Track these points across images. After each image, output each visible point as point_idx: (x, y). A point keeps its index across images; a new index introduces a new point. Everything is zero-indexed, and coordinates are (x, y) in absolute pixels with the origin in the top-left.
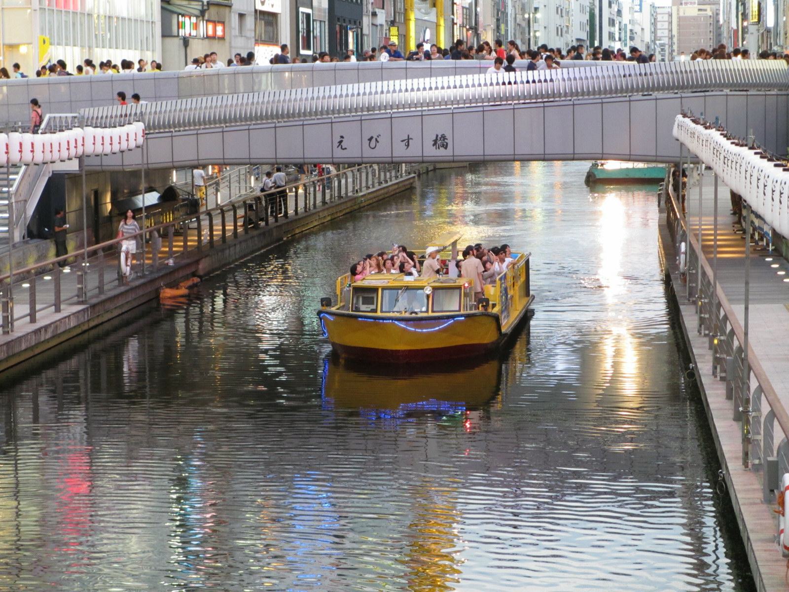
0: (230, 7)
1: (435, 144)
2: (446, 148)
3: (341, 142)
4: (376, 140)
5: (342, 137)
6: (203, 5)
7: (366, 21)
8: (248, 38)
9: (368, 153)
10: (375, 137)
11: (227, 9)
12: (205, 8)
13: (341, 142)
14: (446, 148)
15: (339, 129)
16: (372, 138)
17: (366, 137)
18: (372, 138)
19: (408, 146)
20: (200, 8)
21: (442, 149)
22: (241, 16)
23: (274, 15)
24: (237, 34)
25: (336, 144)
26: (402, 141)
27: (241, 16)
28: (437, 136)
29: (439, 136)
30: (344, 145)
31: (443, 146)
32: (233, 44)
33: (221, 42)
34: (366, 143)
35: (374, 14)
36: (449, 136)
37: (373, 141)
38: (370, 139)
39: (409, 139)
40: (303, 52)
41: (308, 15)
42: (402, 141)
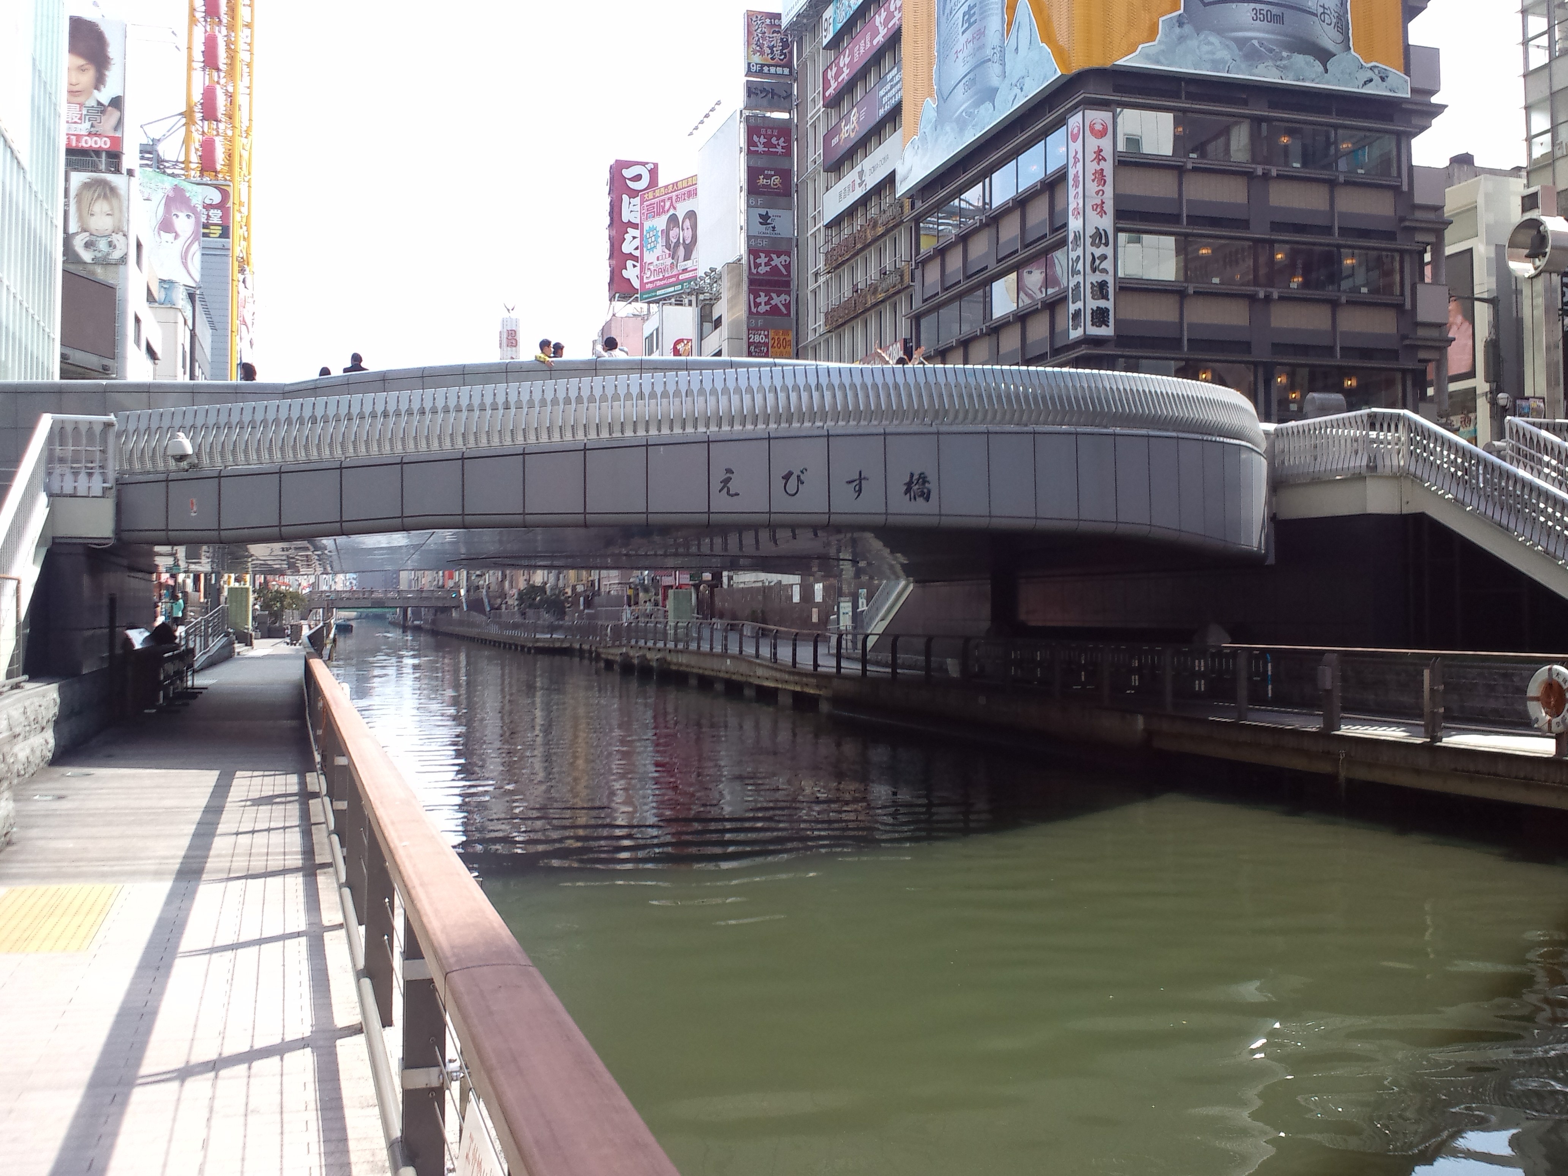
1: (908, 491)
2: (927, 499)
3: (726, 481)
4: (798, 477)
5: (729, 471)
9: (783, 504)
10: (796, 473)
13: (726, 481)
14: (927, 499)
15: (722, 457)
16: (790, 474)
17: (778, 473)
18: (790, 474)
19: (860, 491)
21: (920, 500)
25: (716, 485)
26: (850, 482)
28: (912, 475)
29: (916, 477)
30: (733, 486)
31: (922, 494)
34: (778, 483)
36: (932, 477)
37: (793, 482)
38: (787, 477)
39: (860, 479)
42: (850, 482)
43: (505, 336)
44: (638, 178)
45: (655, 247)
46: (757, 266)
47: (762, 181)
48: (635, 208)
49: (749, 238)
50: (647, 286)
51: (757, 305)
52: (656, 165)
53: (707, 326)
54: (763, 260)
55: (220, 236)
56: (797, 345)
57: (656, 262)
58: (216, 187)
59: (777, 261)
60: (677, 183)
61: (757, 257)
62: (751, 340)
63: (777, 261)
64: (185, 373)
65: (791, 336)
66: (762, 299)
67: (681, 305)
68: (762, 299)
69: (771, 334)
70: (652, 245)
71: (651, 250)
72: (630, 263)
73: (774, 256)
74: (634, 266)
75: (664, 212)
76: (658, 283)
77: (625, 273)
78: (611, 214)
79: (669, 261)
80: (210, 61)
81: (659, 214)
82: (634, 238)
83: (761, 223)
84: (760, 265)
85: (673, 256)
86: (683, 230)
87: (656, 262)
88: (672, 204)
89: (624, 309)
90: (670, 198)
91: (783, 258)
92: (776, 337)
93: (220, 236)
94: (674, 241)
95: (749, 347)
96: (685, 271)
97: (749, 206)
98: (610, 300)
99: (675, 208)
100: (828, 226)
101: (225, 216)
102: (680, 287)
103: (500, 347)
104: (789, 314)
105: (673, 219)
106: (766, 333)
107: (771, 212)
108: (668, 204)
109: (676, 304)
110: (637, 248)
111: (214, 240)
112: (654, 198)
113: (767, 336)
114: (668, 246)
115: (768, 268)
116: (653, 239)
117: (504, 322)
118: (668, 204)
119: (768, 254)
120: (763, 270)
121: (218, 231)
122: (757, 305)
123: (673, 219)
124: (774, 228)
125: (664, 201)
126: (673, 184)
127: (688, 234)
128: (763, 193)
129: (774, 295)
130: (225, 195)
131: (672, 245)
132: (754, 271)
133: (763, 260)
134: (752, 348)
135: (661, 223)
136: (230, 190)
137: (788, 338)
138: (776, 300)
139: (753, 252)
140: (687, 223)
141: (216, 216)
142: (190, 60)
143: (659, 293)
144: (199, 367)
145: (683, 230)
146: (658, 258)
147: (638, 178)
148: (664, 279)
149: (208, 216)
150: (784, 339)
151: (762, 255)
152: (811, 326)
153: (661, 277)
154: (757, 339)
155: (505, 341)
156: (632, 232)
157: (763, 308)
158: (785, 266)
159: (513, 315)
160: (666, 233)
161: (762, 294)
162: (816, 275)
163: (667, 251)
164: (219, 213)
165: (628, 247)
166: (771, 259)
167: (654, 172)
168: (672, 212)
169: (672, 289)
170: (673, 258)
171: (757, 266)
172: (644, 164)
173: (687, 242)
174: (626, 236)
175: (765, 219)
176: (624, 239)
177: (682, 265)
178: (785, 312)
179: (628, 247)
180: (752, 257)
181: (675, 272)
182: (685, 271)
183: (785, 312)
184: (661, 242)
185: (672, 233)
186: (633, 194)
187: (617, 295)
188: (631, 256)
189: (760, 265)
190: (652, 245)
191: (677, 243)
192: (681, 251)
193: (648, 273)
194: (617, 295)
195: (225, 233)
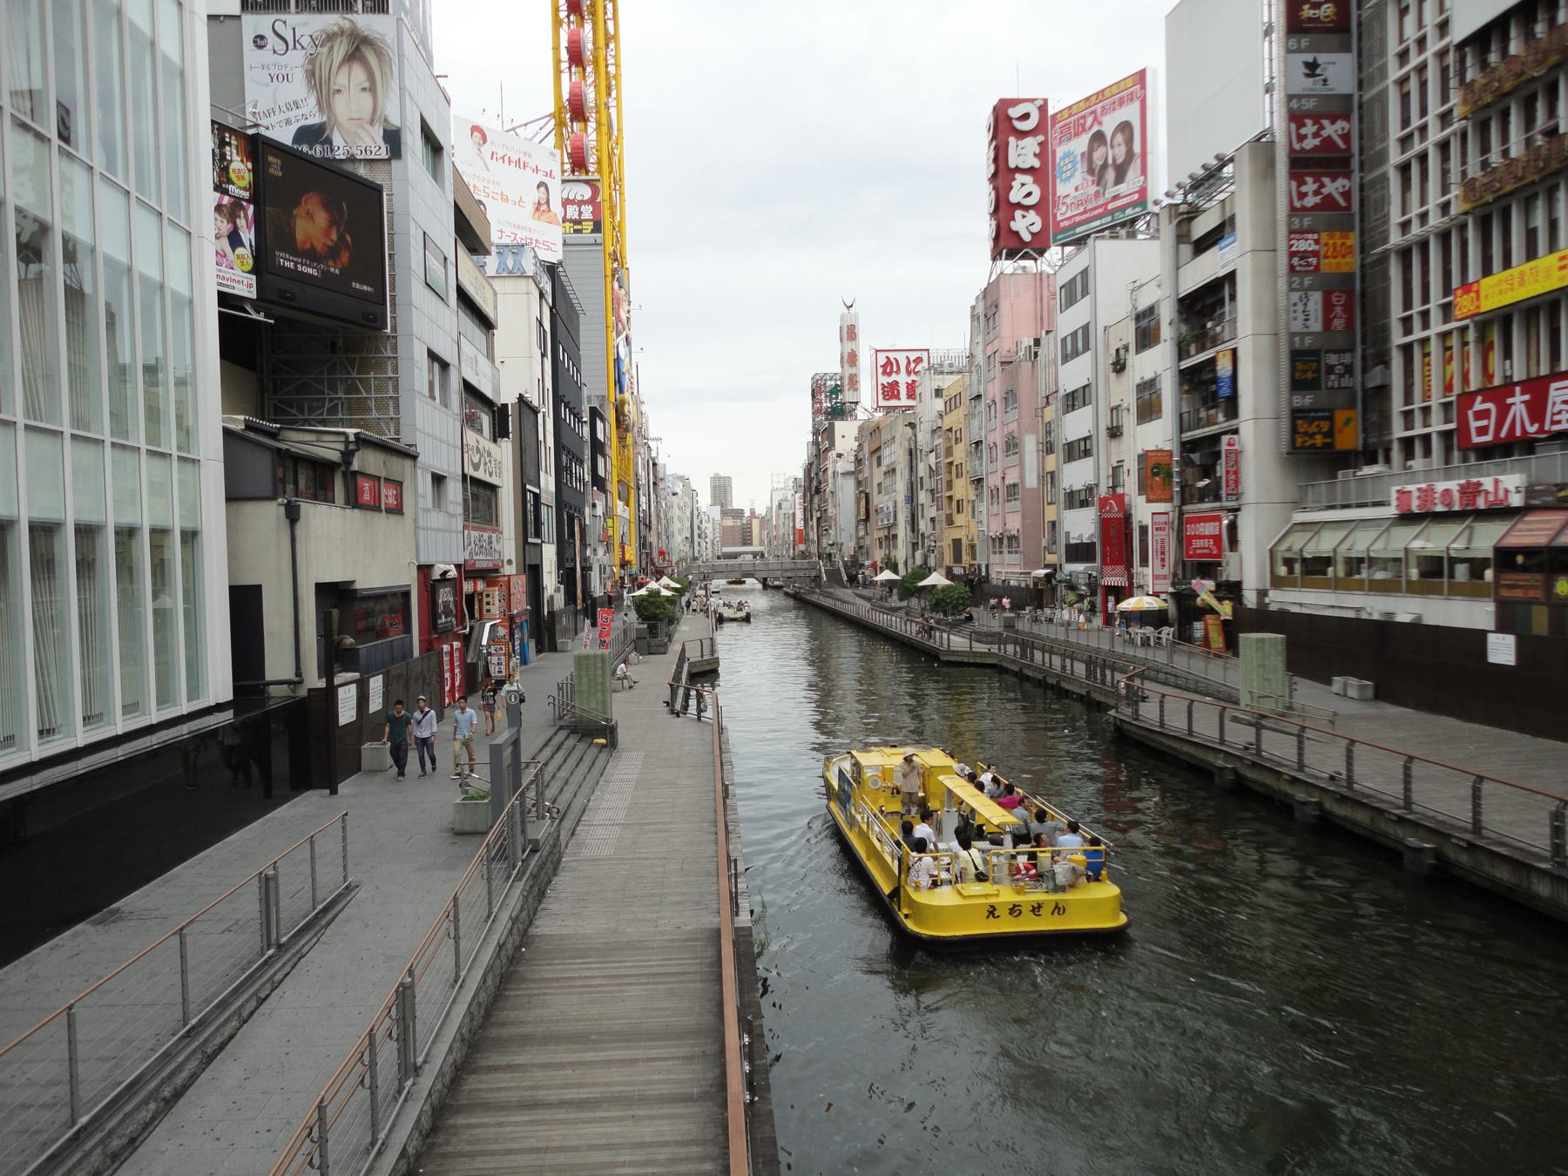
0: (414, 458)
6: (347, 442)
7: (587, 510)
8: (451, 516)
11: (408, 463)
12: (352, 447)
20: (341, 447)
22: (438, 480)
23: (493, 488)
24: (430, 505)
27: (438, 480)
32: (421, 524)
33: (394, 518)
35: (594, 506)
40: (530, 540)
41: (535, 494)
43: (845, 330)
44: (1026, 116)
45: (1072, 175)
46: (1301, 138)
47: (1307, 12)
48: (1023, 151)
49: (1290, 98)
50: (1062, 225)
51: (1302, 196)
52: (1046, 101)
53: (1186, 249)
54: (1309, 129)
55: (593, 231)
56: (1363, 250)
57: (1074, 194)
58: (586, 182)
59: (1332, 130)
60: (1102, 91)
61: (1301, 125)
62: (1294, 249)
63: (1332, 130)
64: (543, 355)
65: (1354, 239)
66: (1310, 186)
67: (1117, 237)
68: (1310, 186)
69: (1324, 238)
70: (1069, 173)
71: (1068, 179)
72: (1018, 213)
73: (1326, 122)
74: (1024, 217)
75: (1084, 130)
76: (1078, 219)
77: (1014, 226)
78: (996, 160)
79: (1093, 189)
80: (576, 57)
81: (1077, 134)
82: (1023, 185)
83: (1307, 75)
84: (1305, 137)
85: (1100, 181)
86: (1112, 147)
87: (1074, 194)
88: (1095, 119)
89: (1007, 266)
90: (1094, 112)
91: (1340, 124)
92: (1331, 242)
93: (593, 231)
94: (1100, 163)
95: (1290, 259)
96: (1116, 198)
97: (1289, 51)
98: (994, 259)
99: (1100, 123)
100: (1461, 46)
101: (597, 210)
102: (1109, 218)
103: (841, 341)
104: (1349, 208)
105: (1099, 138)
106: (1316, 236)
107: (1322, 58)
108: (1090, 120)
109: (1112, 237)
110: (1029, 194)
111: (588, 236)
112: (1070, 116)
113: (1317, 242)
114: (1091, 171)
115: (1317, 142)
116: (1070, 166)
117: (842, 317)
118: (1090, 120)
119: (1317, 118)
120: (1310, 143)
121: (589, 226)
122: (1302, 196)
123: (1099, 138)
124: (1325, 80)
125: (1084, 117)
126: (1097, 94)
127: (1120, 153)
128: (1306, 31)
129: (1326, 180)
130: (595, 191)
131: (1097, 169)
132: (1297, 146)
133: (1309, 129)
134: (1295, 261)
135: (1081, 144)
136: (599, 184)
137: (1349, 242)
138: (1333, 187)
139: (1296, 118)
140: (1119, 138)
141: (587, 212)
142: (558, 61)
143: (1078, 230)
144: (564, 350)
145: (1112, 147)
146: (1076, 189)
147: (1026, 116)
148: (1085, 212)
149: (580, 213)
150: (1343, 244)
151: (1309, 122)
152: (1395, 217)
153: (1081, 210)
154: (1302, 246)
155: (845, 336)
156: (1020, 178)
157: (1310, 201)
158: (1341, 136)
159: (852, 310)
160: (1088, 156)
161: (1309, 180)
162: (1405, 142)
163: (1090, 178)
164: (590, 208)
165: (1015, 196)
166: (1322, 128)
167: (1043, 109)
168: (1096, 128)
169: (1098, 223)
170: (1098, 185)
171: (1301, 138)
172: (1032, 101)
173: (1120, 161)
174: (1014, 183)
175: (1312, 68)
176: (1011, 188)
177: (1111, 191)
178: (1342, 203)
179: (1015, 196)
180: (1293, 126)
181: (1101, 201)
182: (1116, 198)
183: (1342, 203)
184: (1081, 168)
185: (1098, 156)
186: (1022, 135)
187: (1004, 251)
188: (1019, 206)
189: (1305, 137)
190: (1069, 173)
191: (1105, 166)
192: (1111, 175)
193: (1063, 209)
194: (1004, 251)
195: (597, 228)
